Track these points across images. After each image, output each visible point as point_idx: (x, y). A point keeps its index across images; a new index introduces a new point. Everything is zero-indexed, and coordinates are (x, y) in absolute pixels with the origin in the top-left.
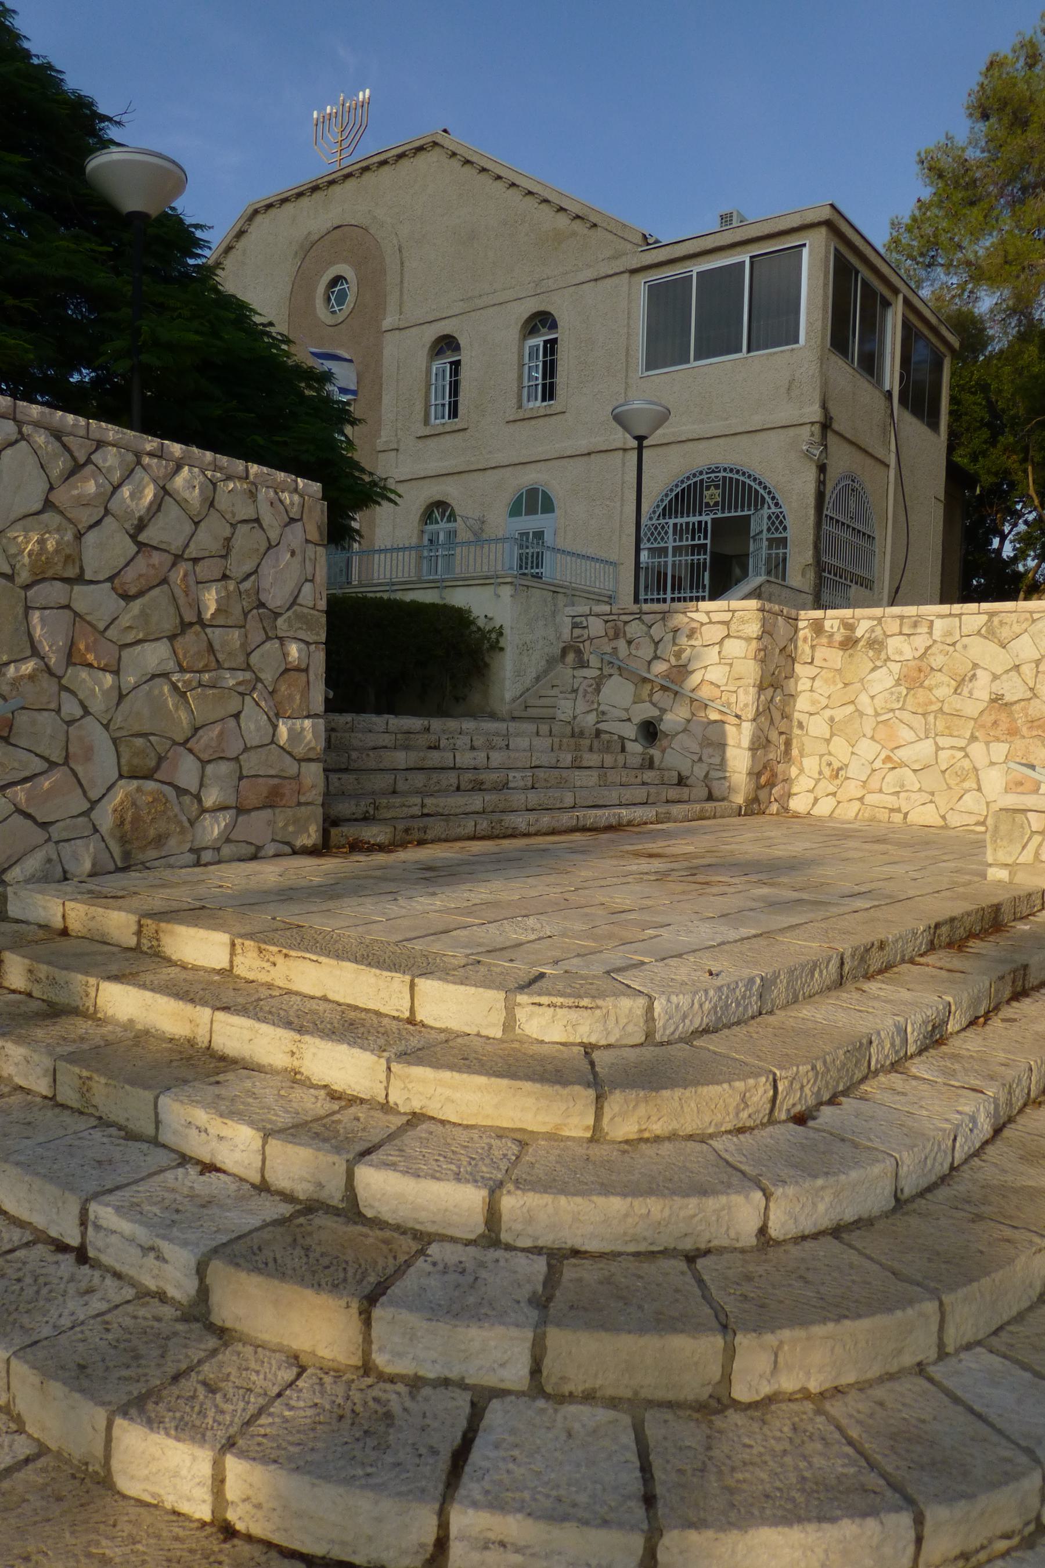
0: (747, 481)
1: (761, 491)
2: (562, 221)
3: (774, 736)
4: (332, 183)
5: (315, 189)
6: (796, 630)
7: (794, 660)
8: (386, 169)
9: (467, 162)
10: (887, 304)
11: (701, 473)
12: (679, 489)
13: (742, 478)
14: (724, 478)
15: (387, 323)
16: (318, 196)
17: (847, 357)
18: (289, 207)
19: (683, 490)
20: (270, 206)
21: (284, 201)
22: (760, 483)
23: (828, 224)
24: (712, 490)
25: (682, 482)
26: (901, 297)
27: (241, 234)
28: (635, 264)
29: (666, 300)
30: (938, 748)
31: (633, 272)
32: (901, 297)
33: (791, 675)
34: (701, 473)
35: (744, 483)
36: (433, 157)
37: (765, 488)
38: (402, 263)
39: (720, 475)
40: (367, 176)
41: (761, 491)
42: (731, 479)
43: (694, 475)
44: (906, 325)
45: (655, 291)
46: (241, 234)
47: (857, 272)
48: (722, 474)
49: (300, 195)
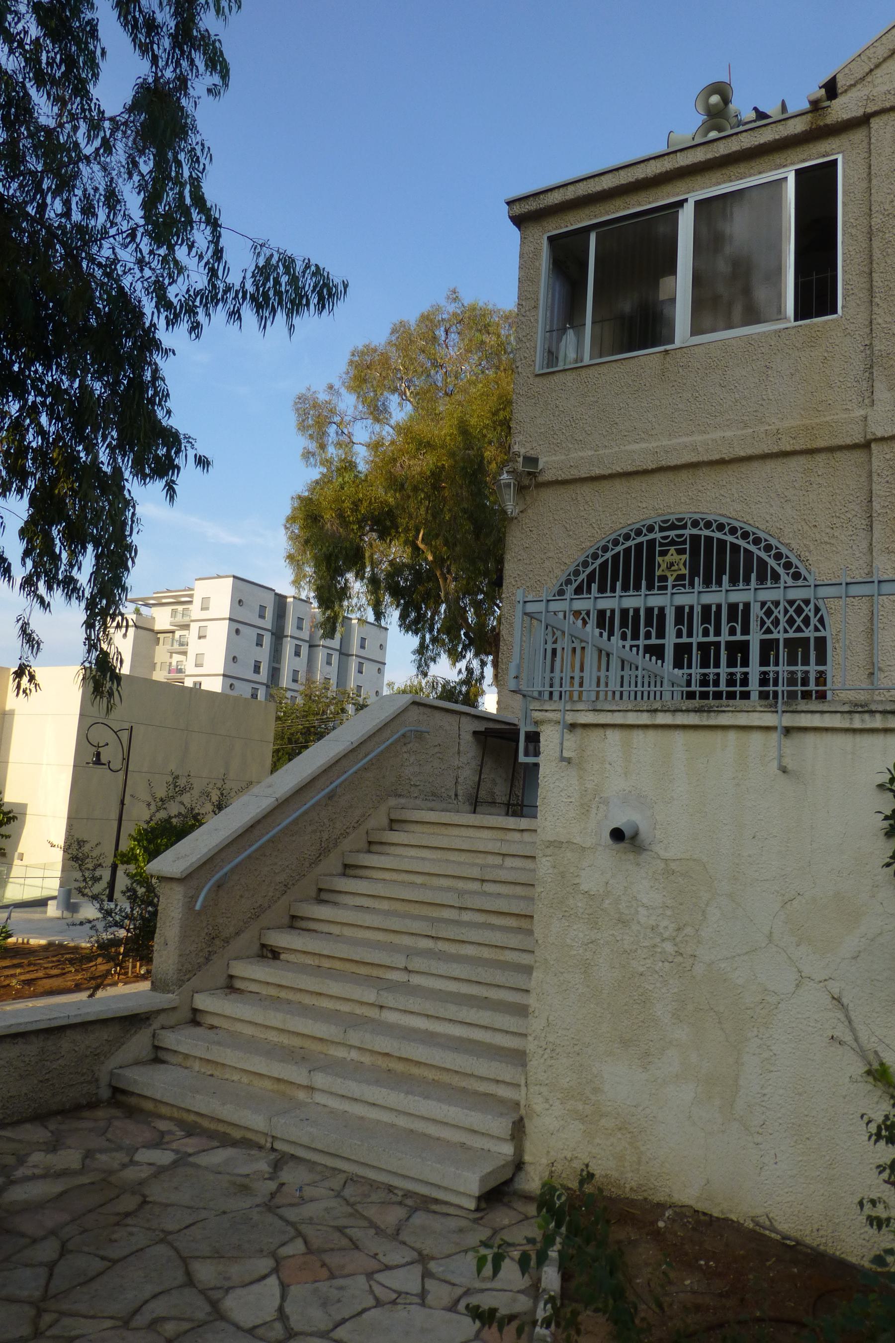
0: (741, 543)
1: (772, 562)
11: (651, 529)
12: (609, 555)
13: (730, 538)
14: (695, 539)
19: (616, 557)
22: (768, 548)
24: (672, 555)
25: (616, 543)
34: (651, 529)
35: (735, 548)
37: (778, 556)
39: (687, 532)
41: (772, 562)
42: (709, 539)
43: (639, 533)
48: (687, 532)
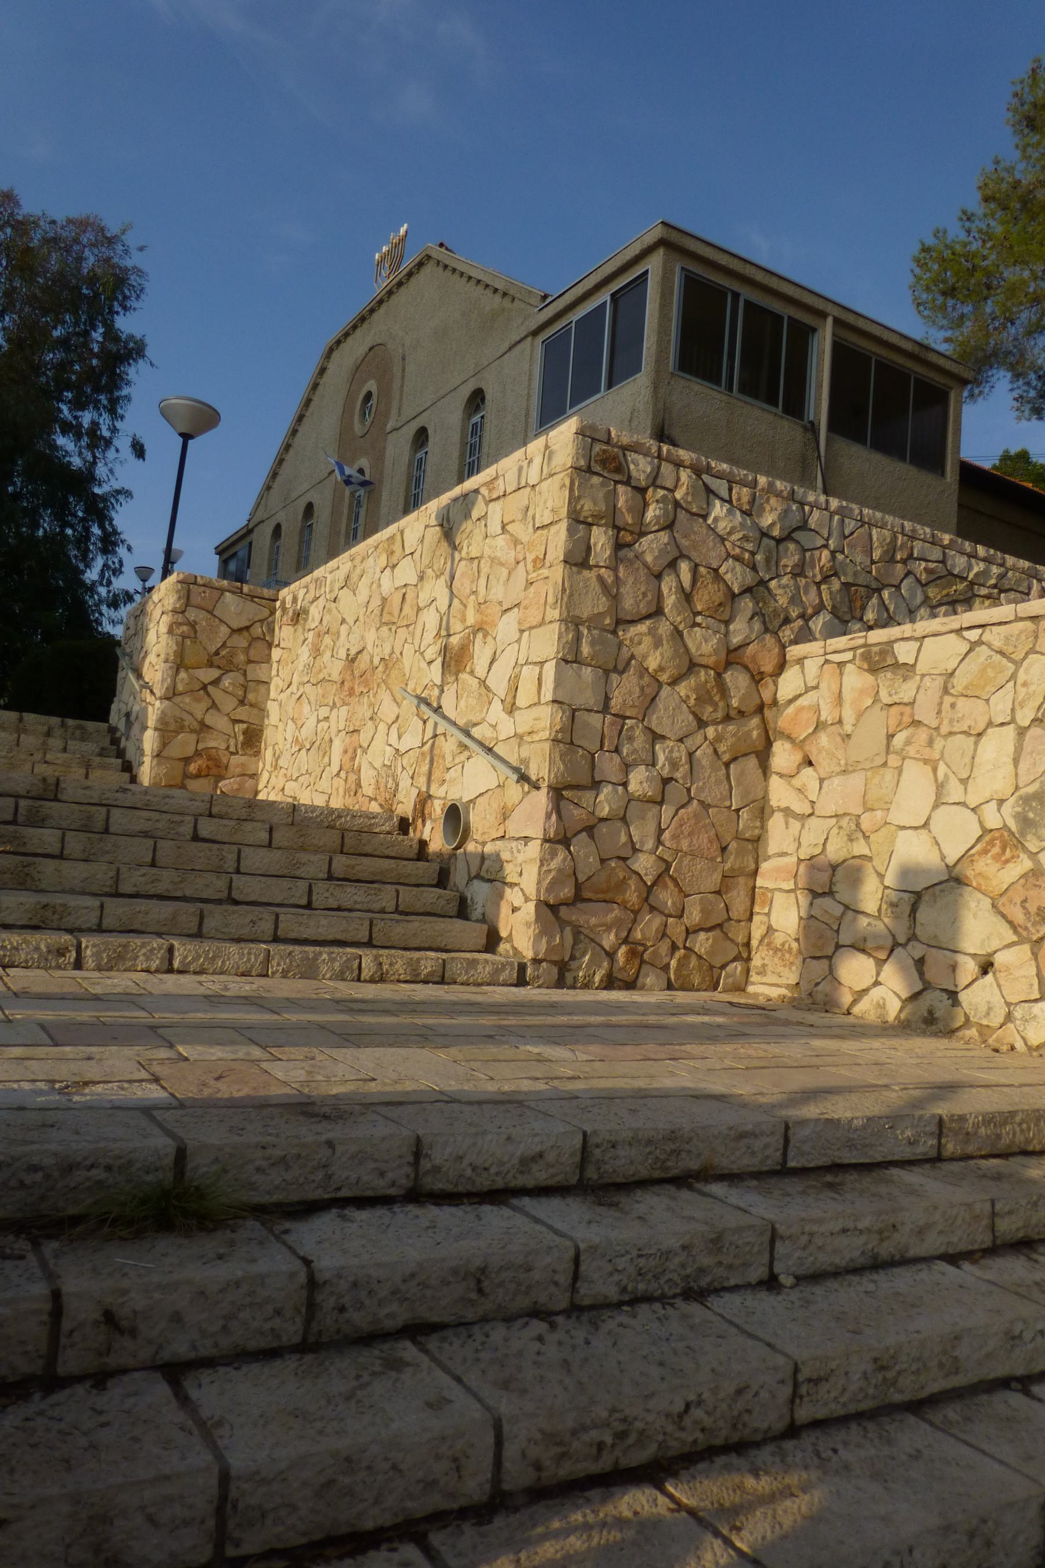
2: (498, 298)
3: (219, 722)
4: (372, 311)
5: (363, 319)
6: (273, 612)
7: (270, 645)
8: (403, 289)
9: (446, 267)
10: (814, 330)
15: (389, 427)
16: (365, 325)
17: (718, 382)
18: (350, 339)
20: (338, 342)
21: (347, 335)
23: (662, 242)
26: (830, 321)
27: (322, 371)
28: (533, 325)
29: (554, 351)
30: (319, 721)
31: (535, 333)
32: (830, 321)
33: (268, 660)
36: (429, 269)
38: (404, 370)
40: (393, 298)
44: (839, 349)
45: (549, 346)
46: (322, 371)
47: (736, 296)
49: (355, 327)
